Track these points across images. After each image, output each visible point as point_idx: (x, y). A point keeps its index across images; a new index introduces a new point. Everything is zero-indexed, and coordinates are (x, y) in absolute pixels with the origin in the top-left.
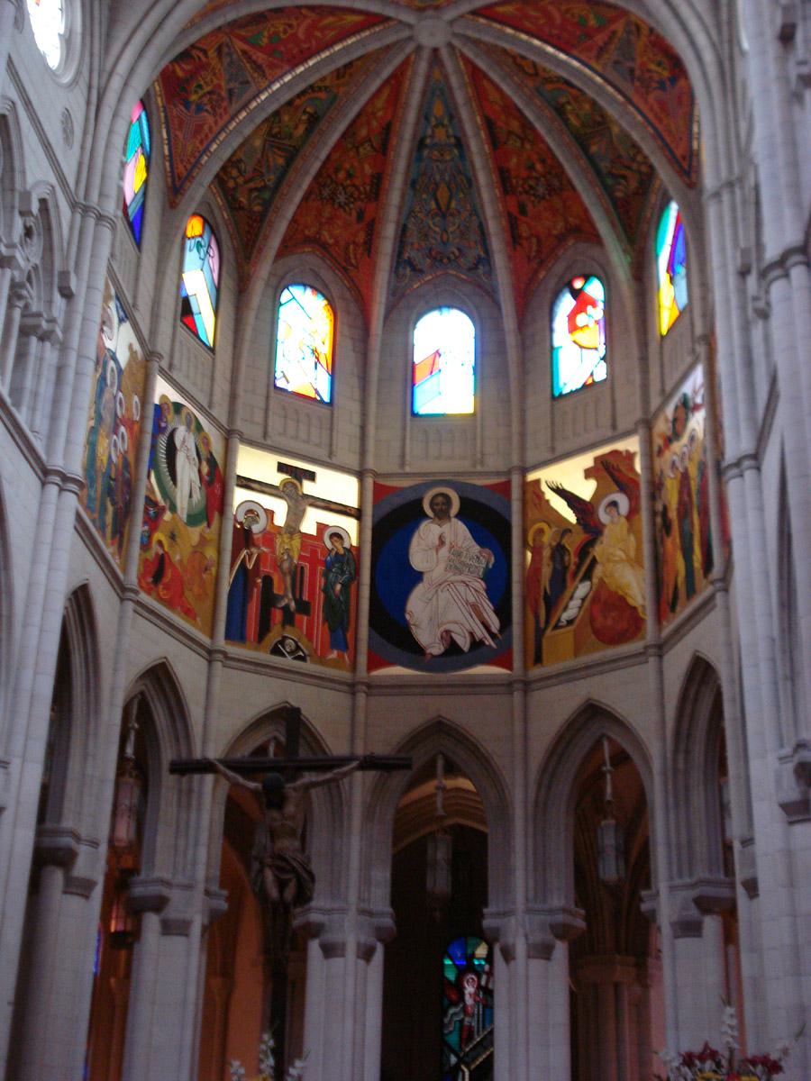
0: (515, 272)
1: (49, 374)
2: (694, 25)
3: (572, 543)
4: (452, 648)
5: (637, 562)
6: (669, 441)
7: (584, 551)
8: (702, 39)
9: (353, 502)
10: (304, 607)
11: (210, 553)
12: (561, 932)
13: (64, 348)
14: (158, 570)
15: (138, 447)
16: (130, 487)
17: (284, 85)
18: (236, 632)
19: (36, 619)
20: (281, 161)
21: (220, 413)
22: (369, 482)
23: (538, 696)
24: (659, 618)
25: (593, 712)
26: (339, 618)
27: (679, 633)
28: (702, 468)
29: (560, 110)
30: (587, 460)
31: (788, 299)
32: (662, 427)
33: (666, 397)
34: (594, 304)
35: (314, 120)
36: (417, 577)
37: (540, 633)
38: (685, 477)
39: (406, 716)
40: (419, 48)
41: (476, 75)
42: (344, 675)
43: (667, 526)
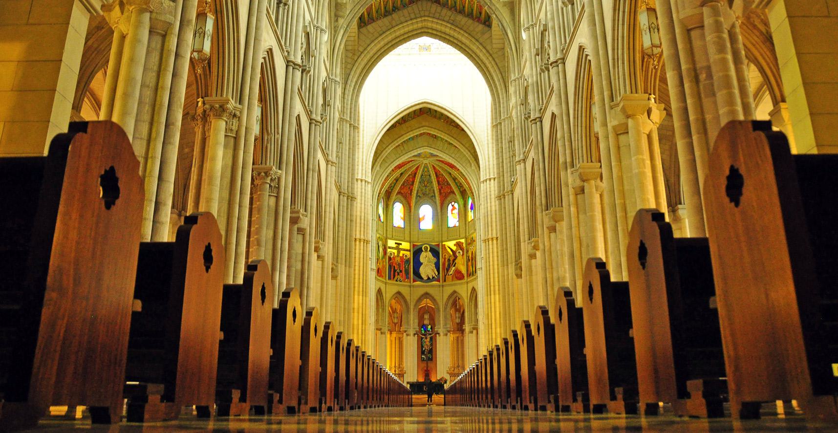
0: (441, 200)
3: (452, 259)
4: (429, 278)
5: (464, 265)
7: (454, 261)
9: (408, 248)
10: (401, 271)
18: (390, 278)
21: (385, 235)
22: (412, 244)
23: (445, 288)
24: (467, 276)
25: (455, 292)
26: (407, 272)
27: (471, 281)
30: (454, 242)
37: (445, 276)
39: (421, 291)
40: (423, 163)
41: (433, 166)
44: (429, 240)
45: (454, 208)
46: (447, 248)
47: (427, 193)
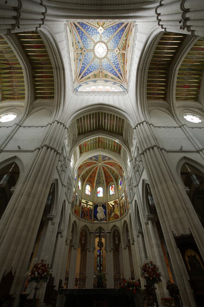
0: (106, 184)
1: (69, 193)
2: (123, 165)
3: (112, 209)
4: (101, 219)
5: (118, 211)
6: (121, 200)
7: (113, 210)
8: (124, 167)
9: (92, 205)
10: (88, 215)
11: (79, 209)
12: (112, 249)
13: (71, 191)
14: (75, 211)
15: (74, 199)
16: (74, 203)
17: (88, 168)
18: (81, 218)
19: (67, 216)
20: (87, 174)
21: (81, 196)
22: (93, 203)
23: (109, 224)
25: (115, 226)
27: (123, 218)
28: (125, 203)
29: (111, 171)
31: (136, 189)
32: (120, 198)
33: (121, 196)
34: (113, 187)
35: (90, 171)
36: (98, 212)
37: (109, 218)
38: (123, 203)
41: (103, 168)
42: (91, 222)
43: (121, 208)
44: (101, 201)
45: (112, 187)
46: (110, 204)
47: (101, 182)
